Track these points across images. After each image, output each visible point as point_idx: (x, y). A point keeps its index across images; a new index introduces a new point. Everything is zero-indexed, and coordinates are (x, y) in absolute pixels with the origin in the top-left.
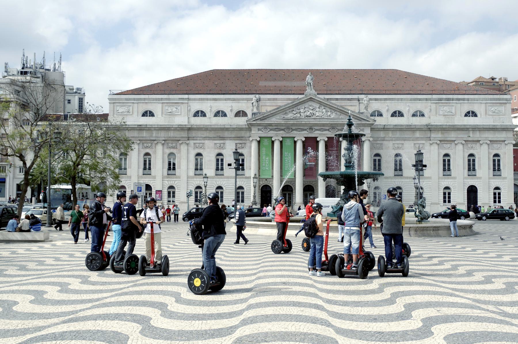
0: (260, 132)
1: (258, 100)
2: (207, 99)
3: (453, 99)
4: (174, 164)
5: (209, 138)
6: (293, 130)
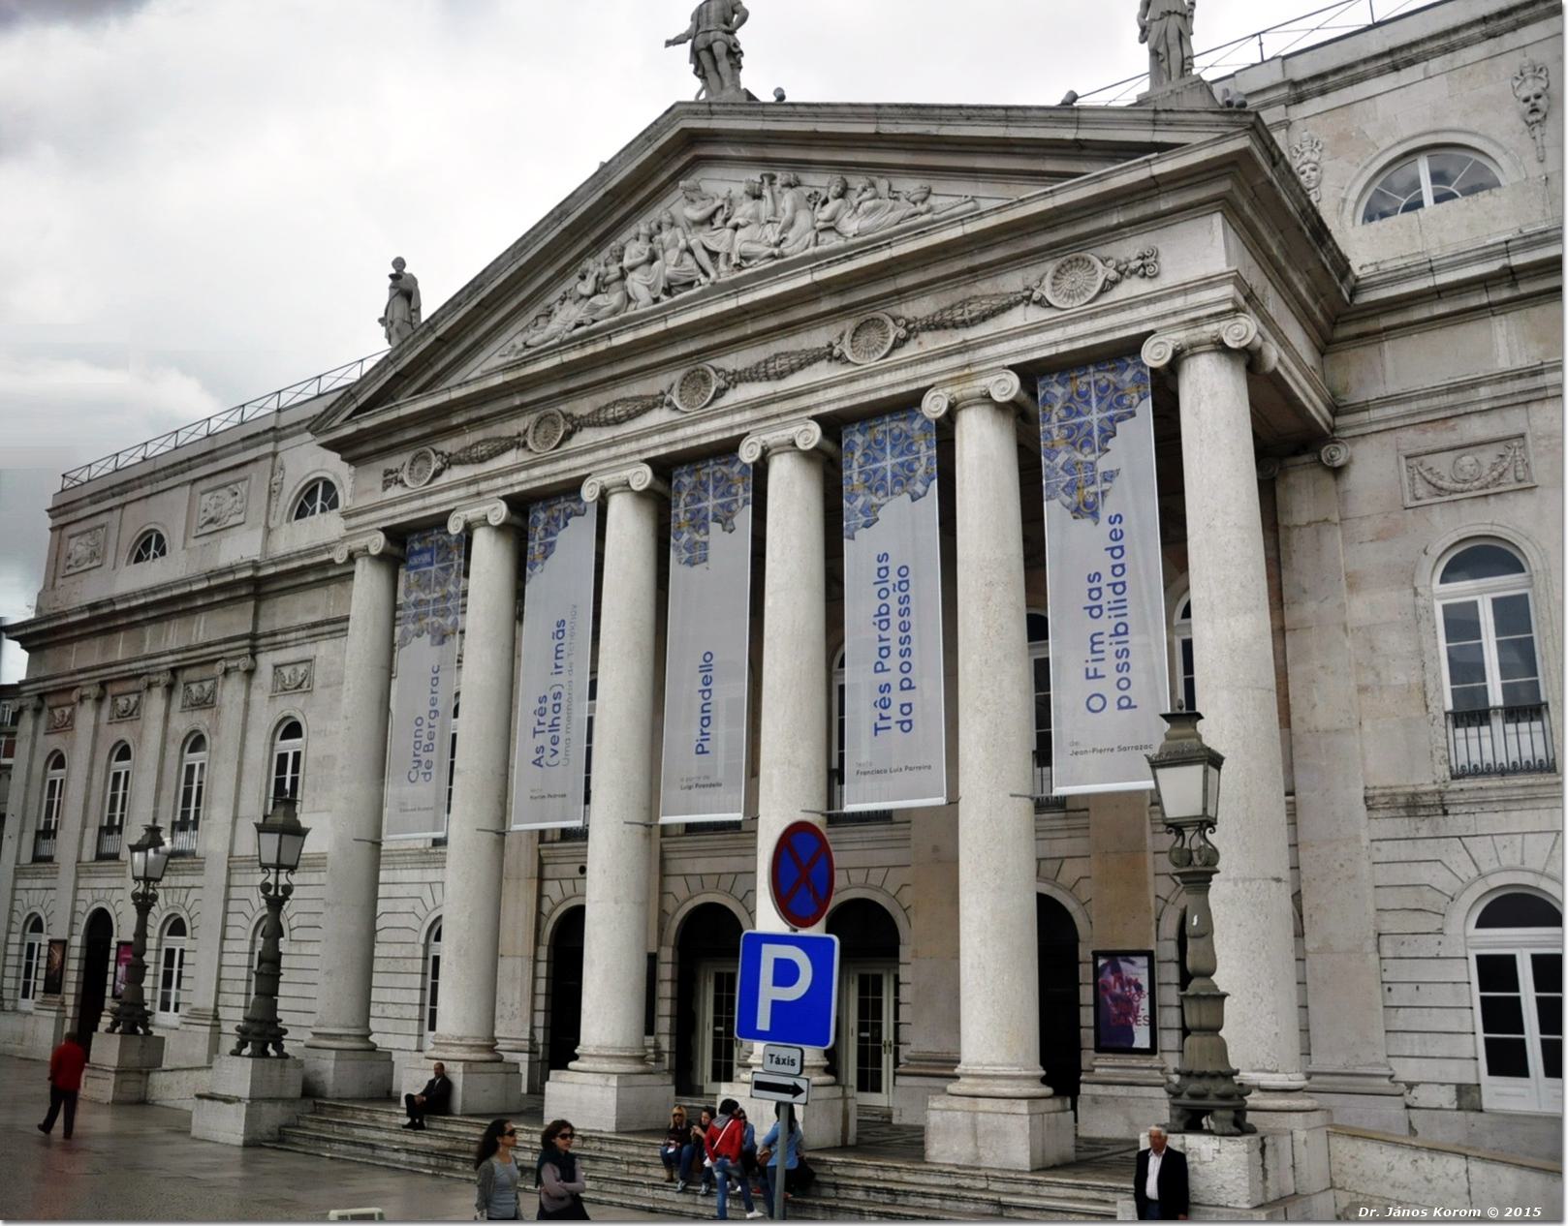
0: (395, 491)
6: (577, 425)
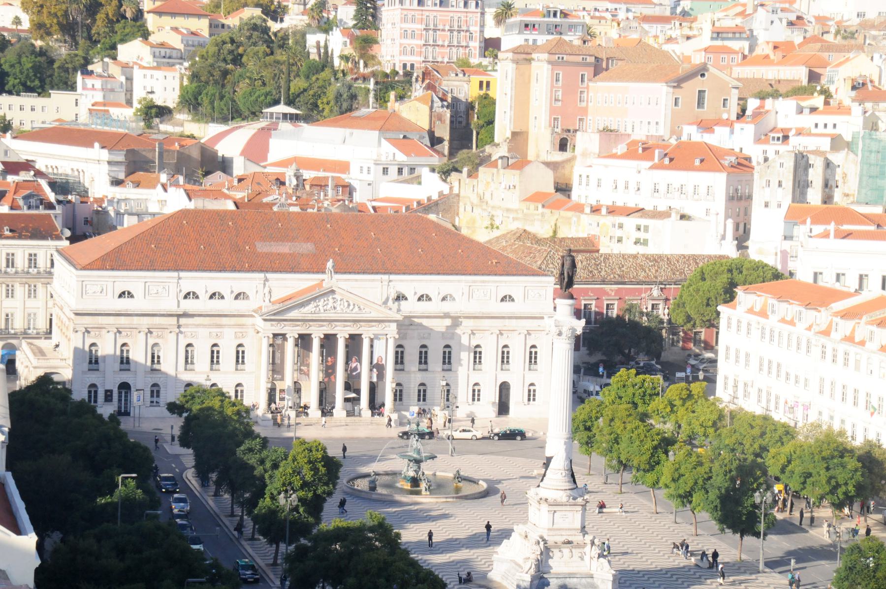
0: (273, 328)
1: (266, 280)
2: (202, 278)
3: (489, 282)
4: (159, 357)
5: (204, 326)
